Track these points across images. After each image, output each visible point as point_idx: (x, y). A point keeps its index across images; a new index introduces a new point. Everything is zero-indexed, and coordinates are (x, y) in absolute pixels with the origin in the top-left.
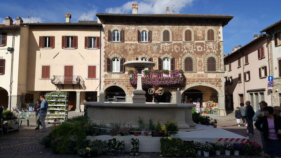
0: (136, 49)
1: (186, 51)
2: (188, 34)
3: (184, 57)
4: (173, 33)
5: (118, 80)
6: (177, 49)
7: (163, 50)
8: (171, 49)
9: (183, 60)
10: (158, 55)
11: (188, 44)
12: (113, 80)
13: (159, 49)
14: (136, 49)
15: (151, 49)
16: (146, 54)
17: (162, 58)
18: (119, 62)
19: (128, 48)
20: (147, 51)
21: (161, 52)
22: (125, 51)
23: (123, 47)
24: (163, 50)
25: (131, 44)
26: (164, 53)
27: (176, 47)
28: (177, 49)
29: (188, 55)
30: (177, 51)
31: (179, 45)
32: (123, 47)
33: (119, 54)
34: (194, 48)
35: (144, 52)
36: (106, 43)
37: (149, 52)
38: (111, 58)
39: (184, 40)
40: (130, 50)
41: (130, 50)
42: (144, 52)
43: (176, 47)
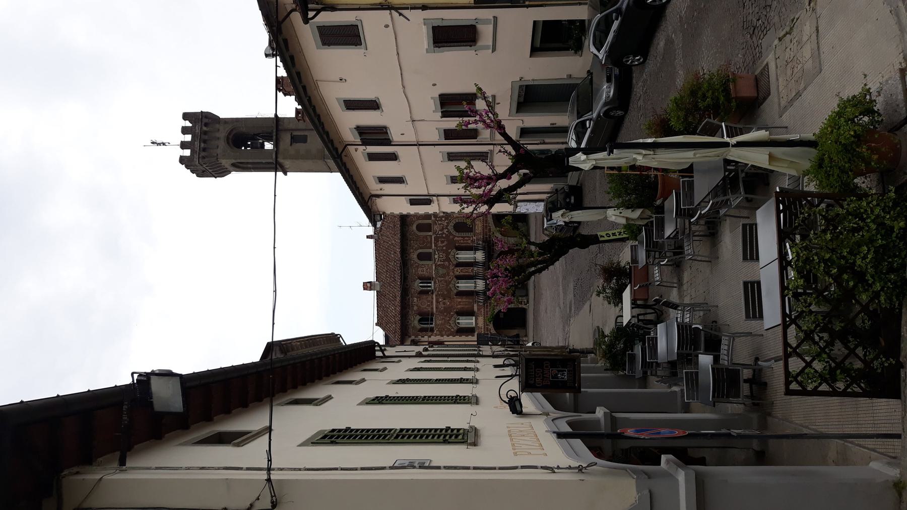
1: (445, 231)
2: (420, 228)
3: (454, 233)
4: (421, 248)
6: (442, 242)
8: (442, 250)
9: (457, 234)
10: (452, 267)
11: (436, 228)
13: (443, 266)
15: (444, 276)
16: (450, 282)
19: (441, 306)
20: (446, 281)
21: (446, 263)
22: (447, 310)
25: (437, 302)
26: (448, 259)
27: (440, 244)
28: (442, 242)
29: (451, 228)
30: (445, 243)
31: (436, 239)
34: (441, 220)
35: (447, 285)
36: (436, 335)
37: (447, 278)
39: (430, 233)
40: (444, 303)
41: (444, 303)
42: (447, 285)
43: (440, 244)
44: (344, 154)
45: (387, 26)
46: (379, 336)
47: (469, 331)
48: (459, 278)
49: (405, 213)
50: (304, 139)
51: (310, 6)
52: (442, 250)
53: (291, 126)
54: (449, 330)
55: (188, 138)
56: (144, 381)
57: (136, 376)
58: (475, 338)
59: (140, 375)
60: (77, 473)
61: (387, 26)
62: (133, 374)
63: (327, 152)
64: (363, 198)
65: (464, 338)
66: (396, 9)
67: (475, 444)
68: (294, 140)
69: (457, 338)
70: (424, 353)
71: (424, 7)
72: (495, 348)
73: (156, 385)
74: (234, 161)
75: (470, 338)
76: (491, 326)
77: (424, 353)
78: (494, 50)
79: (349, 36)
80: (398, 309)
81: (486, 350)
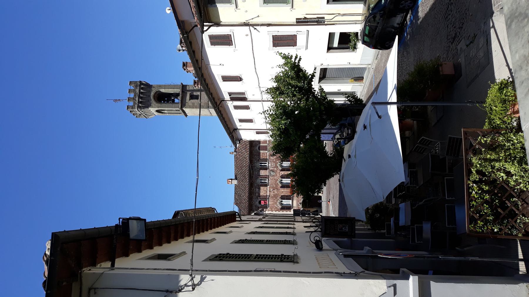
0: (273, 187)
5: (298, 201)
7: (274, 167)
8: (273, 161)
10: (278, 171)
12: (298, 205)
13: (273, 171)
14: (273, 187)
16: (277, 180)
17: (280, 168)
18: (283, 201)
19: (272, 194)
20: (275, 179)
21: (275, 169)
22: (275, 196)
23: (272, 197)
24: (274, 167)
25: (270, 191)
26: (277, 167)
32: (272, 197)
33: (277, 201)
36: (269, 211)
38: (280, 207)
40: (274, 192)
44: (220, 105)
45: (247, 35)
46: (236, 209)
47: (288, 208)
48: (283, 177)
49: (253, 139)
50: (196, 97)
51: (205, 24)
52: (273, 161)
53: (191, 88)
54: (276, 208)
55: (132, 95)
56: (126, 222)
57: (121, 220)
58: (292, 212)
59: (123, 219)
60: (90, 270)
61: (247, 35)
62: (119, 219)
63: (210, 105)
64: (230, 130)
65: (285, 212)
66: (253, 25)
67: (297, 263)
68: (192, 97)
69: (281, 212)
70: (263, 219)
71: (269, 25)
72: (304, 218)
73: (133, 225)
74: (157, 109)
75: (288, 213)
76: (301, 206)
77: (263, 219)
78: (307, 48)
79: (225, 40)
80: (247, 194)
81: (298, 218)
